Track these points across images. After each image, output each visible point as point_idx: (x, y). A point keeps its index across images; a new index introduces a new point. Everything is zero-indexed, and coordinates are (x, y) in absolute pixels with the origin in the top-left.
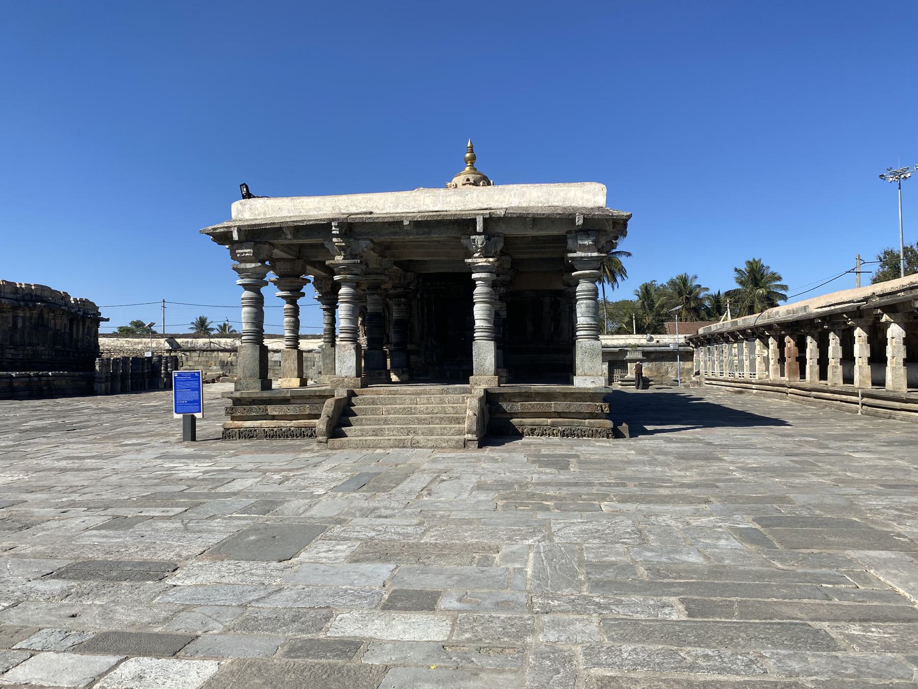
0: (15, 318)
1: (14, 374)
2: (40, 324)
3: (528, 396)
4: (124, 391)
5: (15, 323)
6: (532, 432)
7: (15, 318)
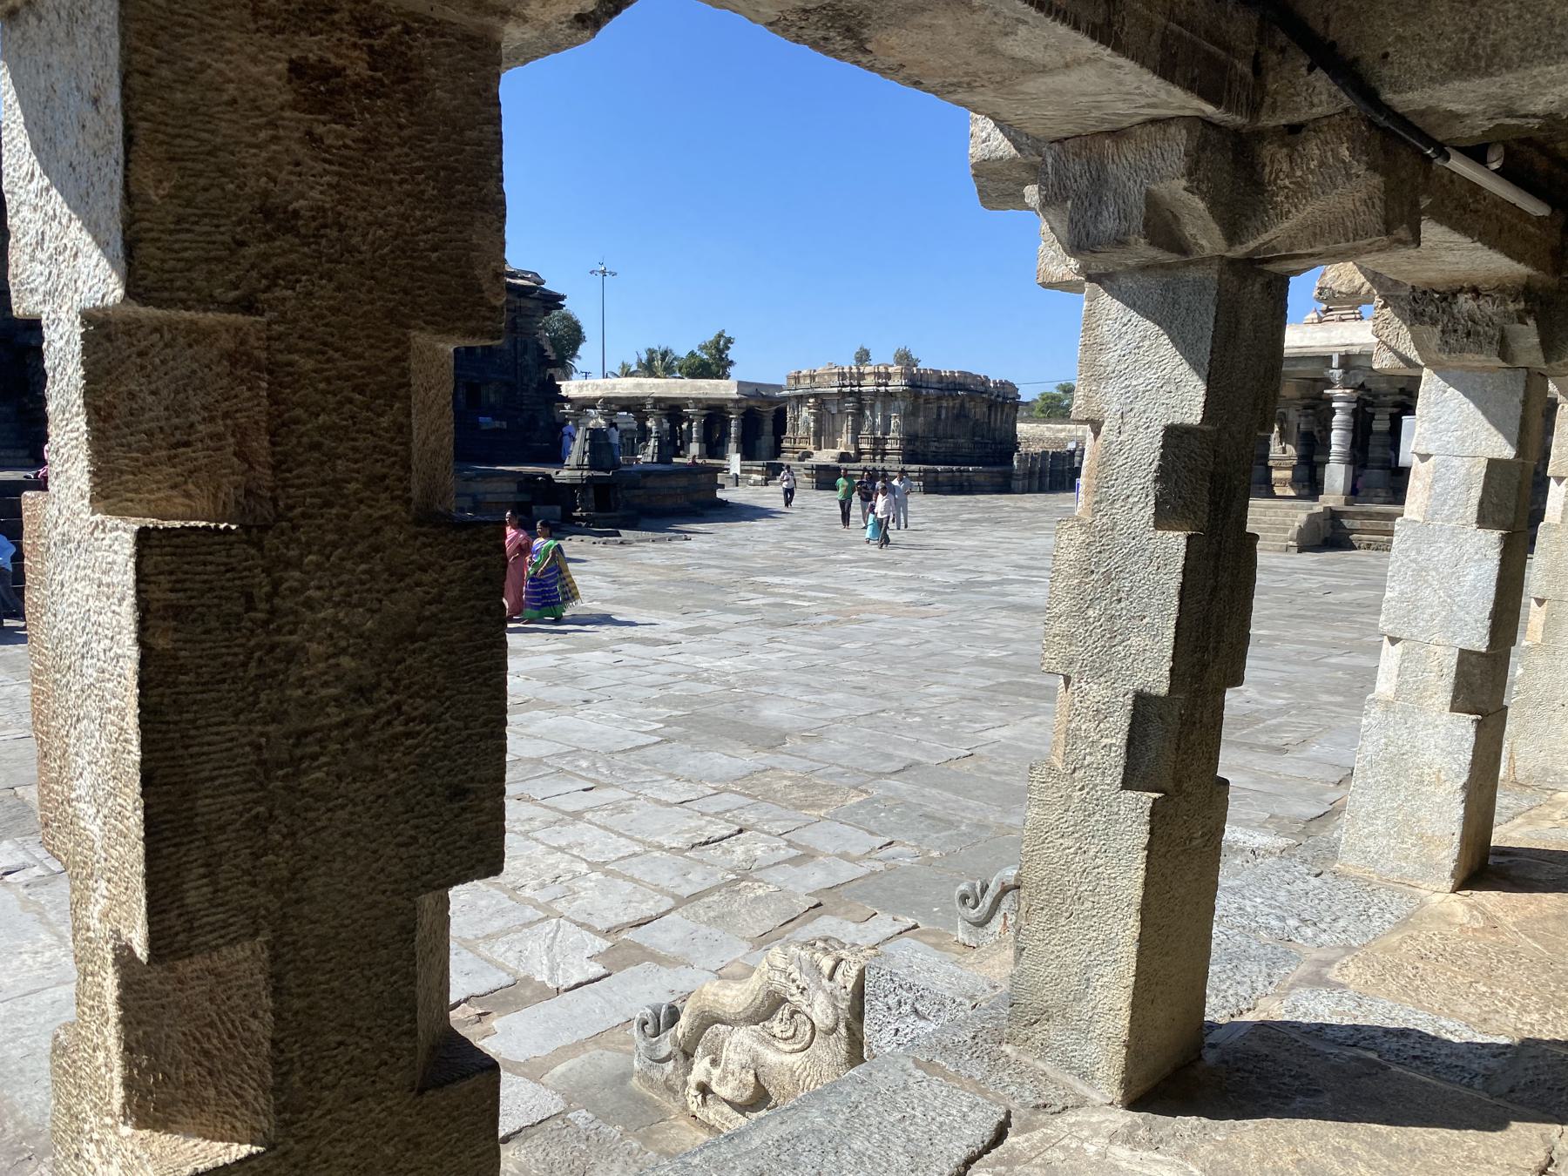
0: (940, 408)
2: (961, 415)
3: (1369, 516)
4: (1041, 491)
5: (939, 415)
6: (1369, 546)
7: (940, 408)
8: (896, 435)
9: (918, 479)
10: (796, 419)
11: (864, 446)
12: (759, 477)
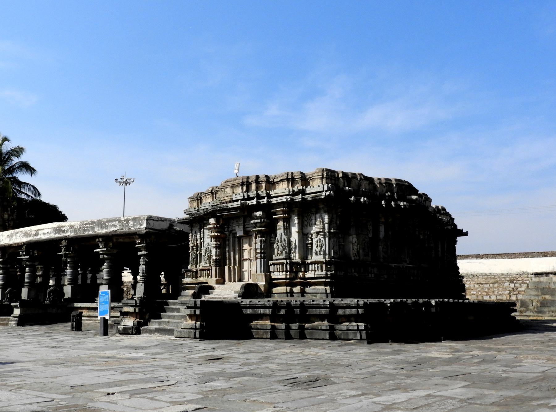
1: (388, 302)
8: (320, 258)
9: (357, 318)
10: (198, 247)
11: (278, 275)
12: (129, 322)
